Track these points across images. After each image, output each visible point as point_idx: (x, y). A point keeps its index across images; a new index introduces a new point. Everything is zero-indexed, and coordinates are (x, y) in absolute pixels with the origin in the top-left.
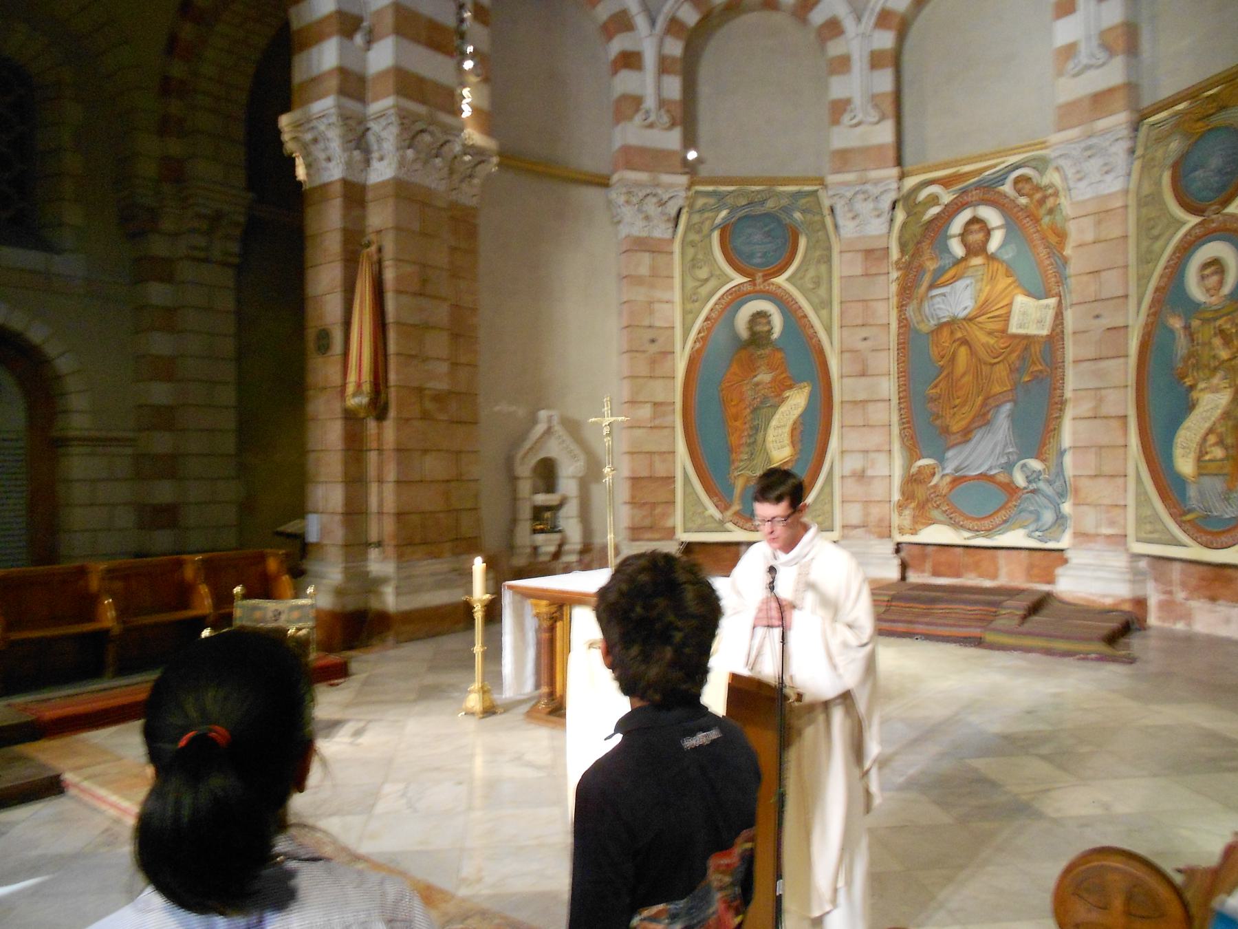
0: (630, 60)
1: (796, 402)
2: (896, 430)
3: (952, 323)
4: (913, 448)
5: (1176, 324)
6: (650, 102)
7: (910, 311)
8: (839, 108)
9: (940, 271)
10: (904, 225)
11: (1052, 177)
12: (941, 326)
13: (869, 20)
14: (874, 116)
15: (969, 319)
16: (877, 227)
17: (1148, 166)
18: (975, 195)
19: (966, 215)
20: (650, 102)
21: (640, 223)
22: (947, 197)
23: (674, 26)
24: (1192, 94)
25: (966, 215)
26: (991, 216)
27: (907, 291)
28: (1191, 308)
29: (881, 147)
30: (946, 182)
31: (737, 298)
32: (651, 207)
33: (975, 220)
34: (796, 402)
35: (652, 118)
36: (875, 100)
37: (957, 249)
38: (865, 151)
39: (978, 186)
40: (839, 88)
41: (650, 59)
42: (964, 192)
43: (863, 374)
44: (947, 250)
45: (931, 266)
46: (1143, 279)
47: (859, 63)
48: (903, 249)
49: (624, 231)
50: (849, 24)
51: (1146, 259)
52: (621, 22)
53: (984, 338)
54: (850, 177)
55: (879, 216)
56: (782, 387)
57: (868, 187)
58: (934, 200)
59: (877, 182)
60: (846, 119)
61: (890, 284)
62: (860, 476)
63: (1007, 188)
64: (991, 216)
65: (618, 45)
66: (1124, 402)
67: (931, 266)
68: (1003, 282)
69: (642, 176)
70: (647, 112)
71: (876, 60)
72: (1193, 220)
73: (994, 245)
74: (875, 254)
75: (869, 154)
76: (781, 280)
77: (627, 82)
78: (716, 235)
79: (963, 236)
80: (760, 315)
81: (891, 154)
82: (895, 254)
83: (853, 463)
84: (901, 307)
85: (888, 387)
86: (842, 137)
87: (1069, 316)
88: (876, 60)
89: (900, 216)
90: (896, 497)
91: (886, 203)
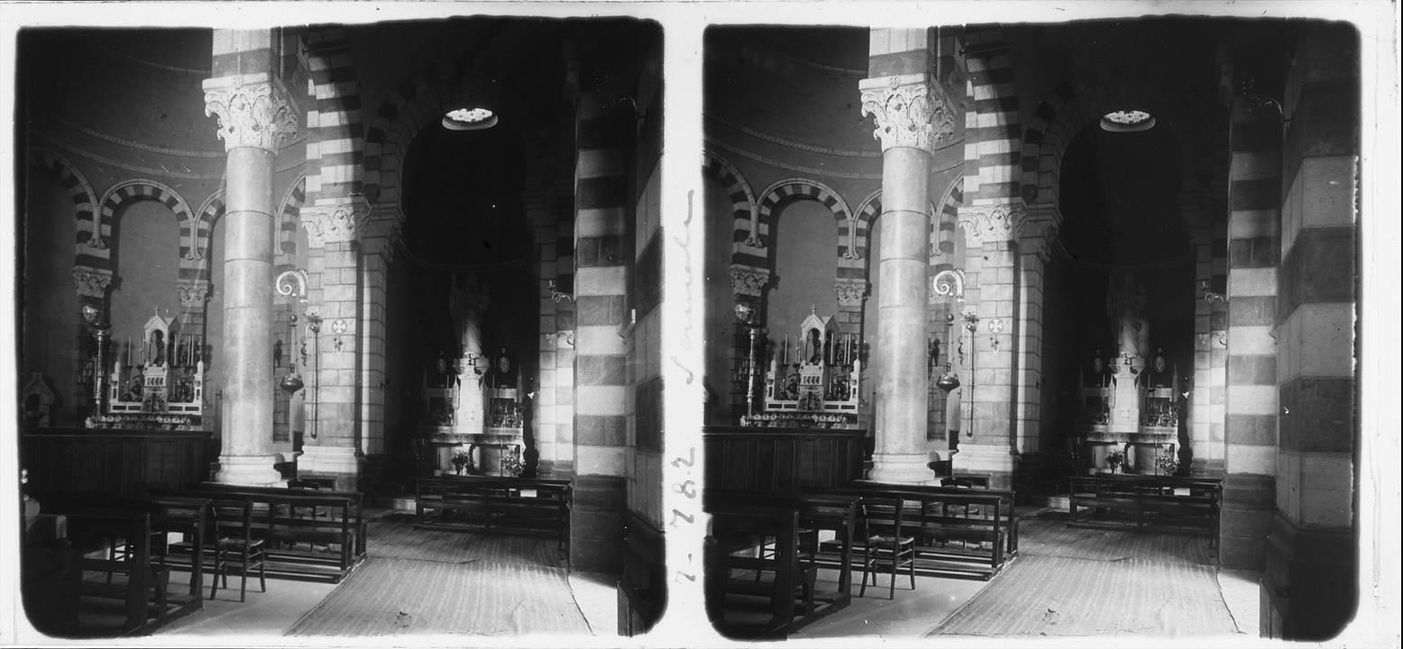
0: (745, 215)
14: (857, 256)
20: (753, 235)
21: (744, 287)
29: (861, 270)
32: (750, 281)
35: (754, 242)
36: (858, 249)
38: (853, 270)
49: (736, 291)
52: (741, 197)
54: (845, 280)
55: (857, 298)
57: (853, 286)
59: (856, 284)
60: (845, 254)
65: (737, 206)
69: (748, 268)
70: (751, 240)
71: (859, 232)
75: (855, 273)
77: (740, 224)
81: (863, 273)
88: (859, 232)
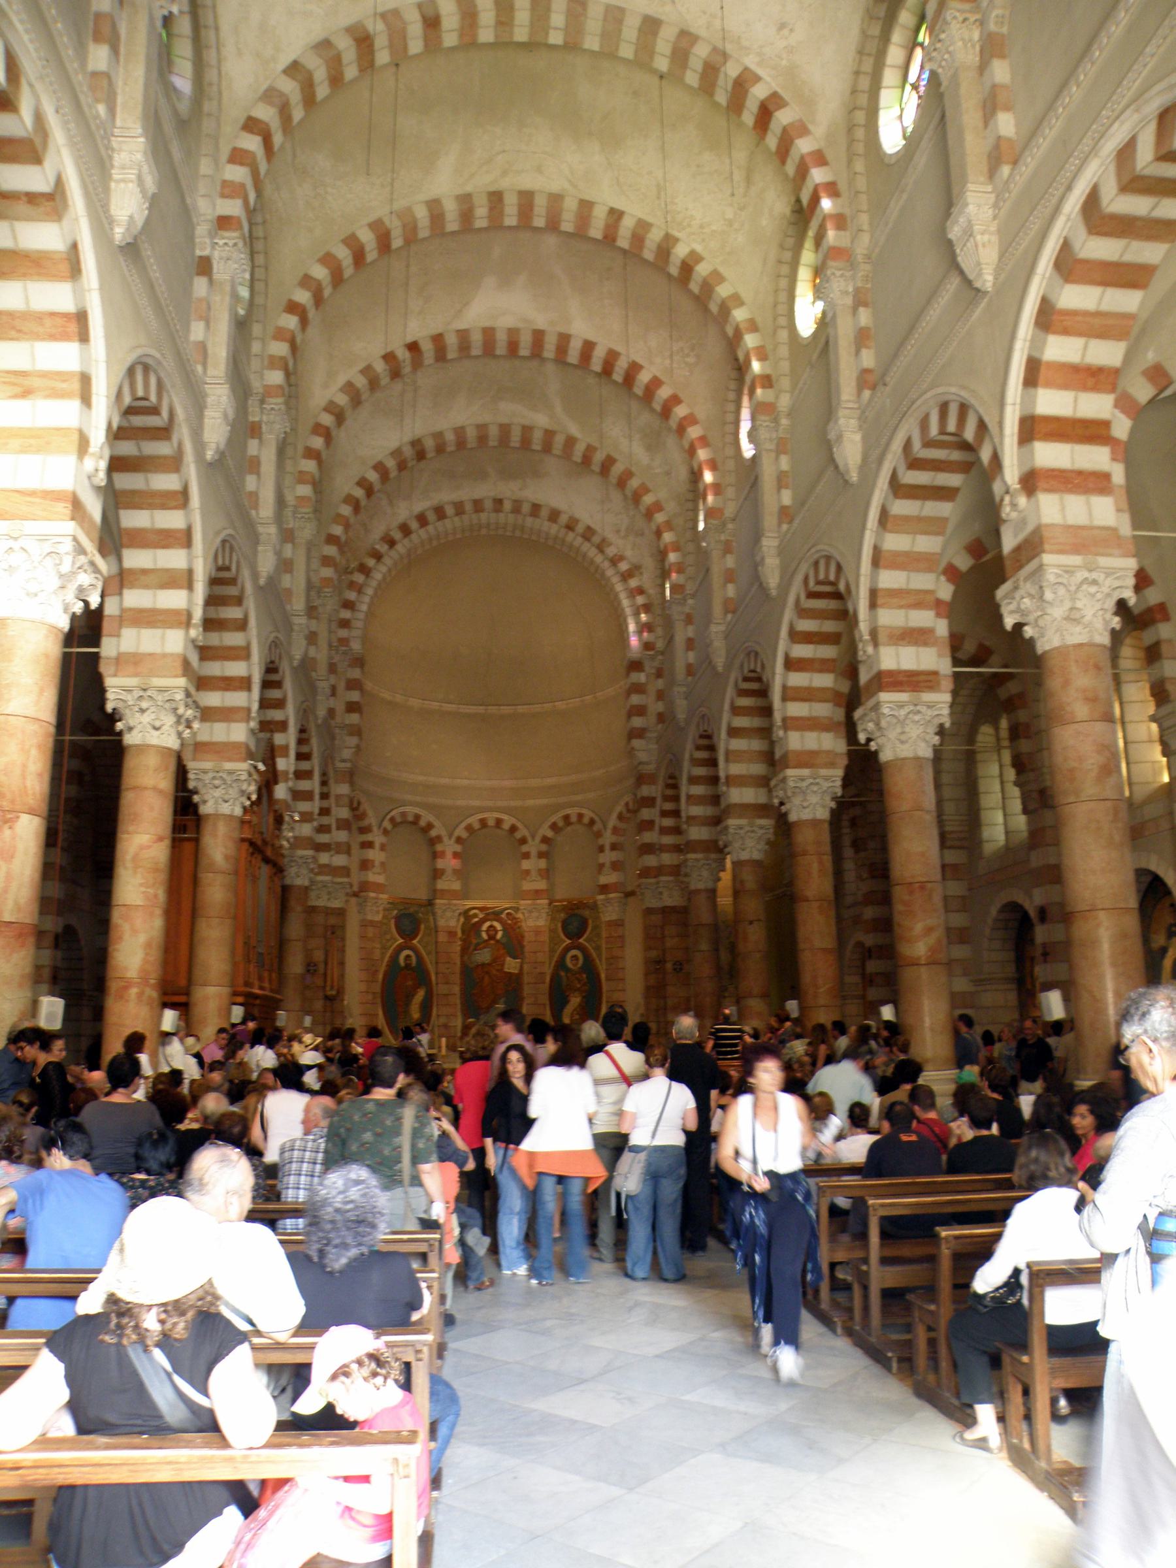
1: (420, 995)
2: (459, 1007)
3: (483, 965)
4: (466, 1015)
5: (563, 974)
6: (377, 863)
7: (466, 958)
8: (437, 874)
9: (478, 944)
10: (464, 924)
11: (520, 915)
12: (478, 966)
13: (453, 839)
15: (489, 964)
16: (453, 923)
17: (553, 919)
18: (492, 917)
19: (488, 924)
22: (481, 916)
23: (386, 832)
24: (569, 901)
25: (488, 924)
26: (498, 926)
27: (464, 950)
28: (568, 970)
30: (481, 909)
31: (400, 948)
33: (491, 926)
34: (420, 995)
37: (485, 936)
39: (494, 913)
40: (440, 864)
41: (377, 845)
42: (487, 914)
43: (447, 983)
44: (480, 936)
45: (474, 941)
46: (551, 957)
47: (449, 855)
48: (463, 932)
50: (445, 839)
51: (552, 951)
53: (494, 972)
56: (416, 987)
58: (475, 916)
60: (444, 877)
61: (457, 947)
62: (446, 1026)
63: (503, 916)
64: (498, 926)
66: (545, 999)
67: (474, 941)
68: (502, 952)
71: (456, 855)
72: (568, 941)
73: (499, 935)
74: (452, 934)
76: (415, 942)
78: (393, 921)
79: (487, 931)
80: (408, 957)
82: (459, 934)
83: (442, 1020)
84: (462, 956)
85: (456, 989)
86: (441, 885)
87: (526, 967)
89: (462, 920)
90: (459, 1034)
91: (456, 914)
